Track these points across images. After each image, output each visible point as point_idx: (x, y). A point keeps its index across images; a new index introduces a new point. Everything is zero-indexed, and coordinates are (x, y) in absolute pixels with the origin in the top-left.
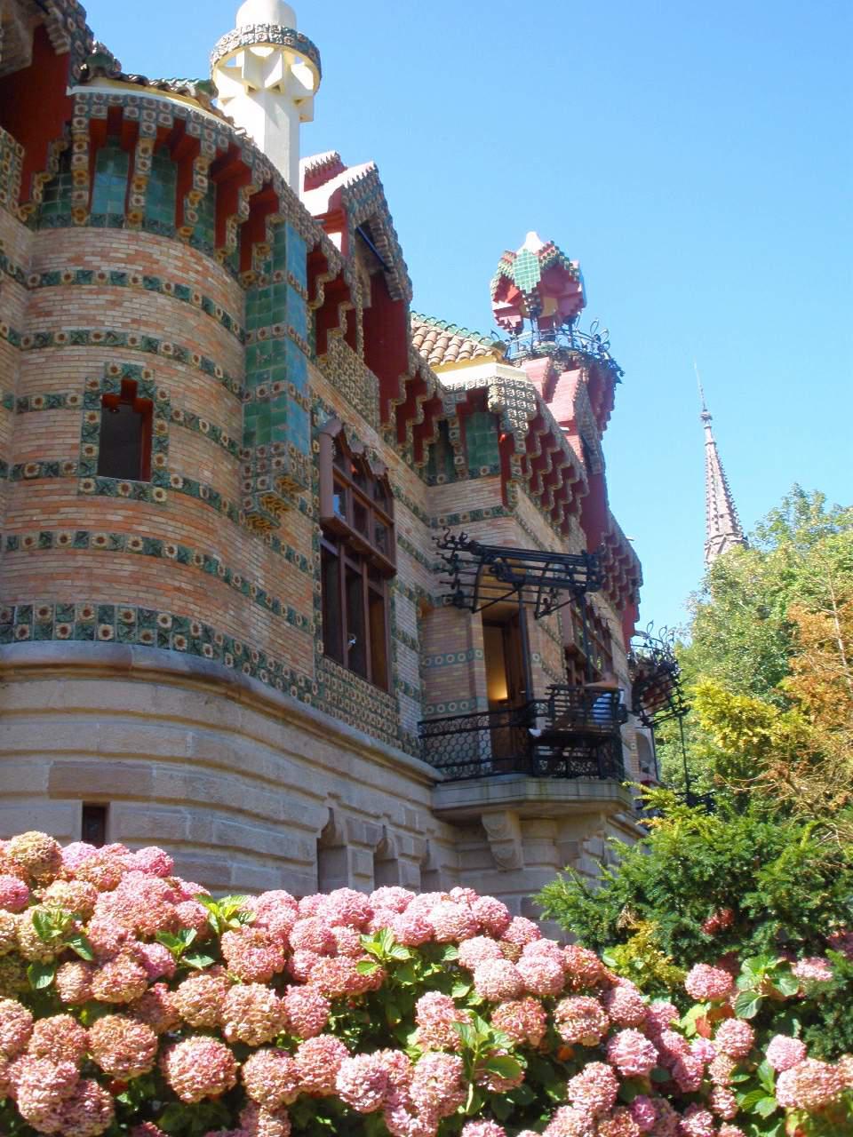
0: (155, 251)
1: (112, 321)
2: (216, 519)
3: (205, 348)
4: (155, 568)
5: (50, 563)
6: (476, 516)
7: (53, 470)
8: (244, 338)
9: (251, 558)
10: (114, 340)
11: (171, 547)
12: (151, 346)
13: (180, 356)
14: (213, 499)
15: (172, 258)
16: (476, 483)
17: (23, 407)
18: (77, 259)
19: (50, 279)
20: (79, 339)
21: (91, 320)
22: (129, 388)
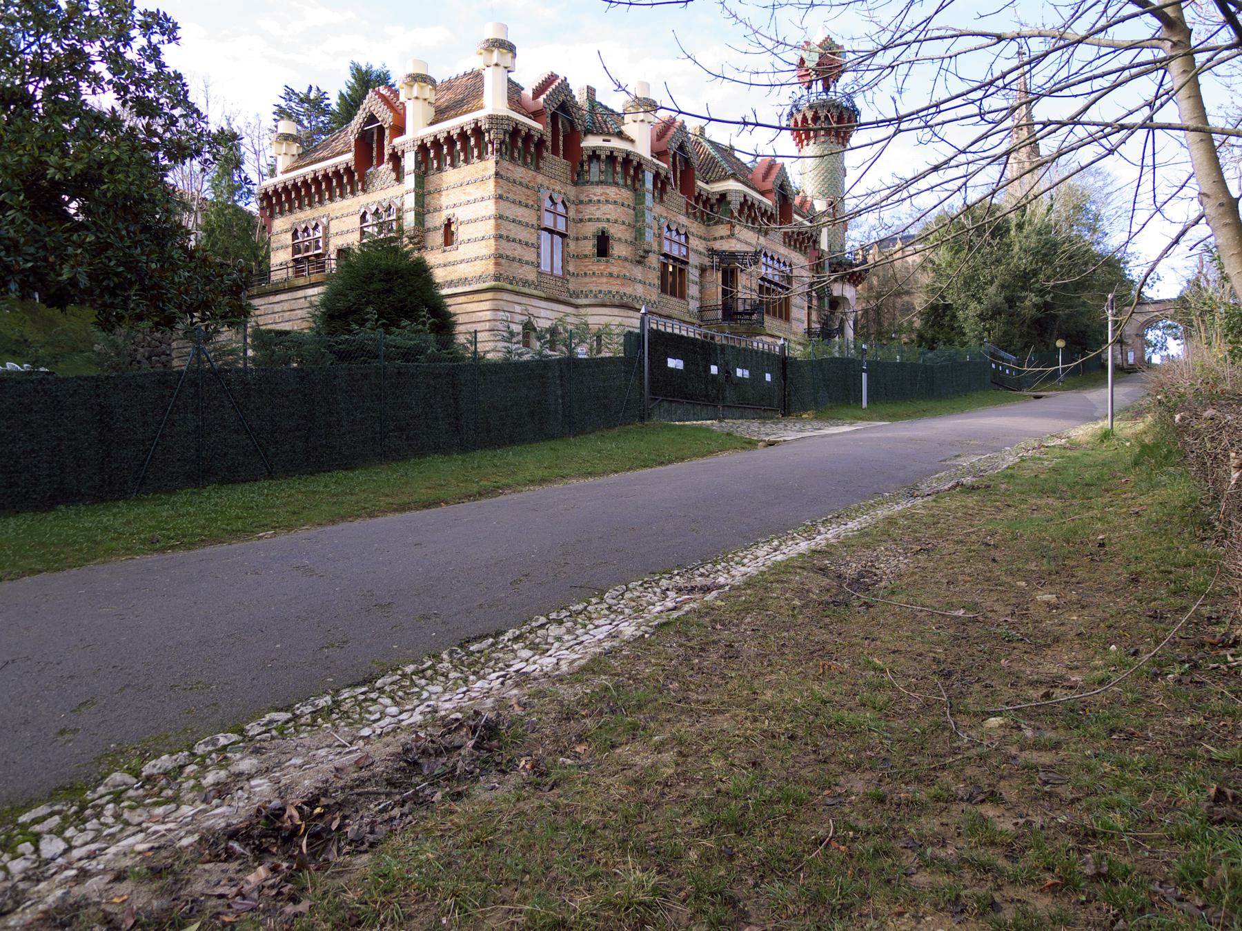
0: (608, 191)
1: (598, 214)
2: (627, 264)
3: (623, 218)
4: (611, 280)
5: (587, 280)
6: (722, 238)
7: (586, 256)
8: (634, 209)
9: (638, 272)
10: (598, 220)
11: (615, 274)
12: (608, 220)
13: (616, 222)
14: (626, 259)
15: (612, 192)
16: (722, 226)
17: (577, 239)
18: (587, 196)
19: (581, 202)
20: (590, 220)
21: (592, 214)
22: (603, 232)
